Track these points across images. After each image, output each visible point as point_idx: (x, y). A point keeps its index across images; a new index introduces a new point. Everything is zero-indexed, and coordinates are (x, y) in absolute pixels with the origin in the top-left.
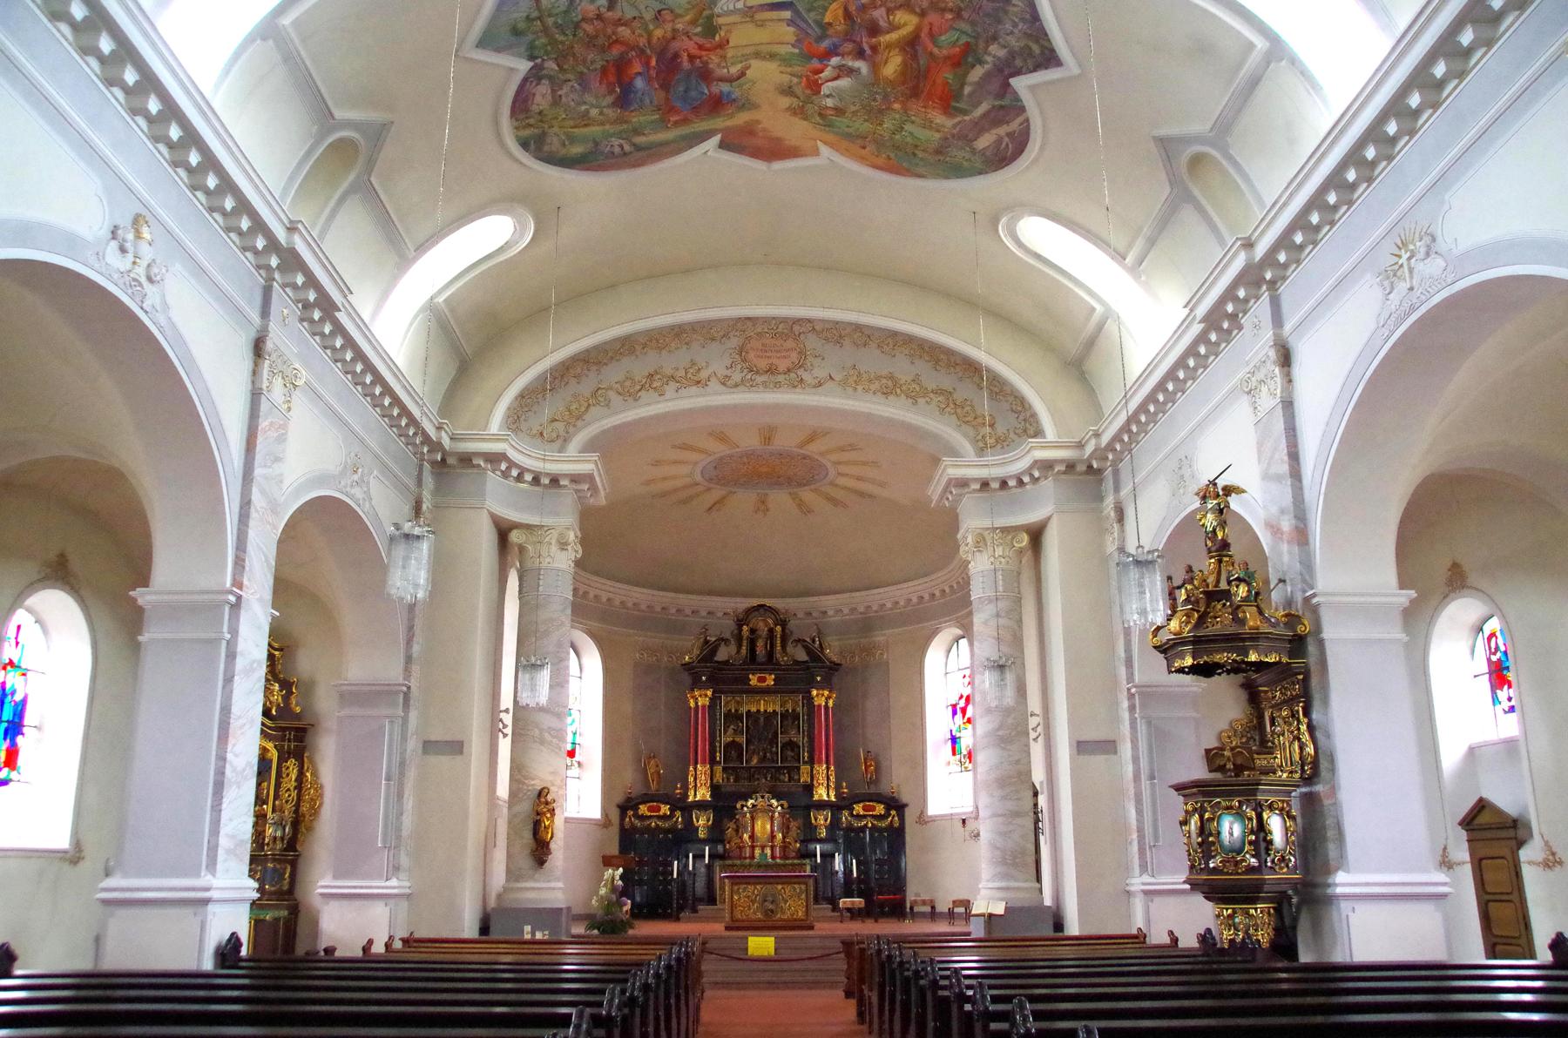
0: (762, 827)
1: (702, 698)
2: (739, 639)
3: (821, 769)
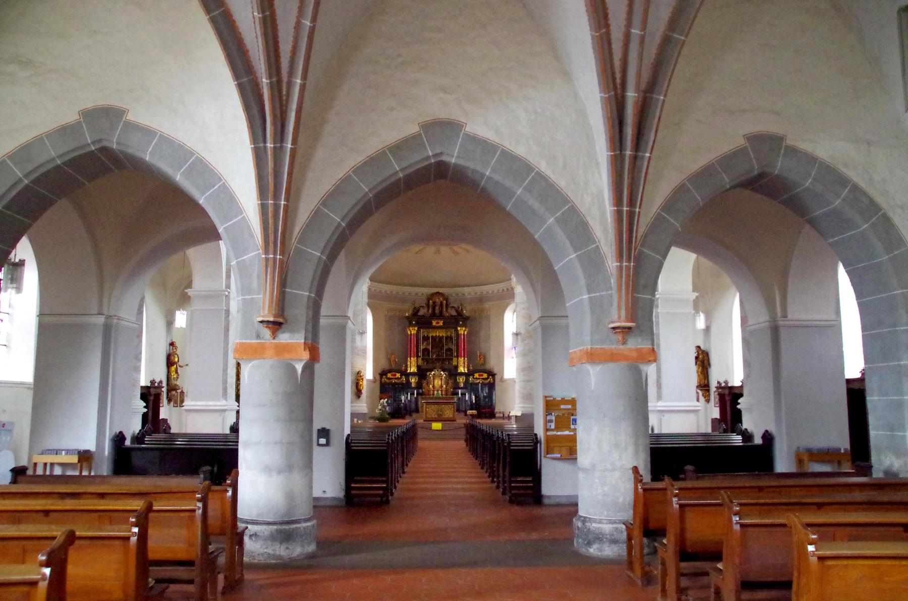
0: (437, 382)
1: (413, 331)
2: (428, 306)
3: (461, 360)
